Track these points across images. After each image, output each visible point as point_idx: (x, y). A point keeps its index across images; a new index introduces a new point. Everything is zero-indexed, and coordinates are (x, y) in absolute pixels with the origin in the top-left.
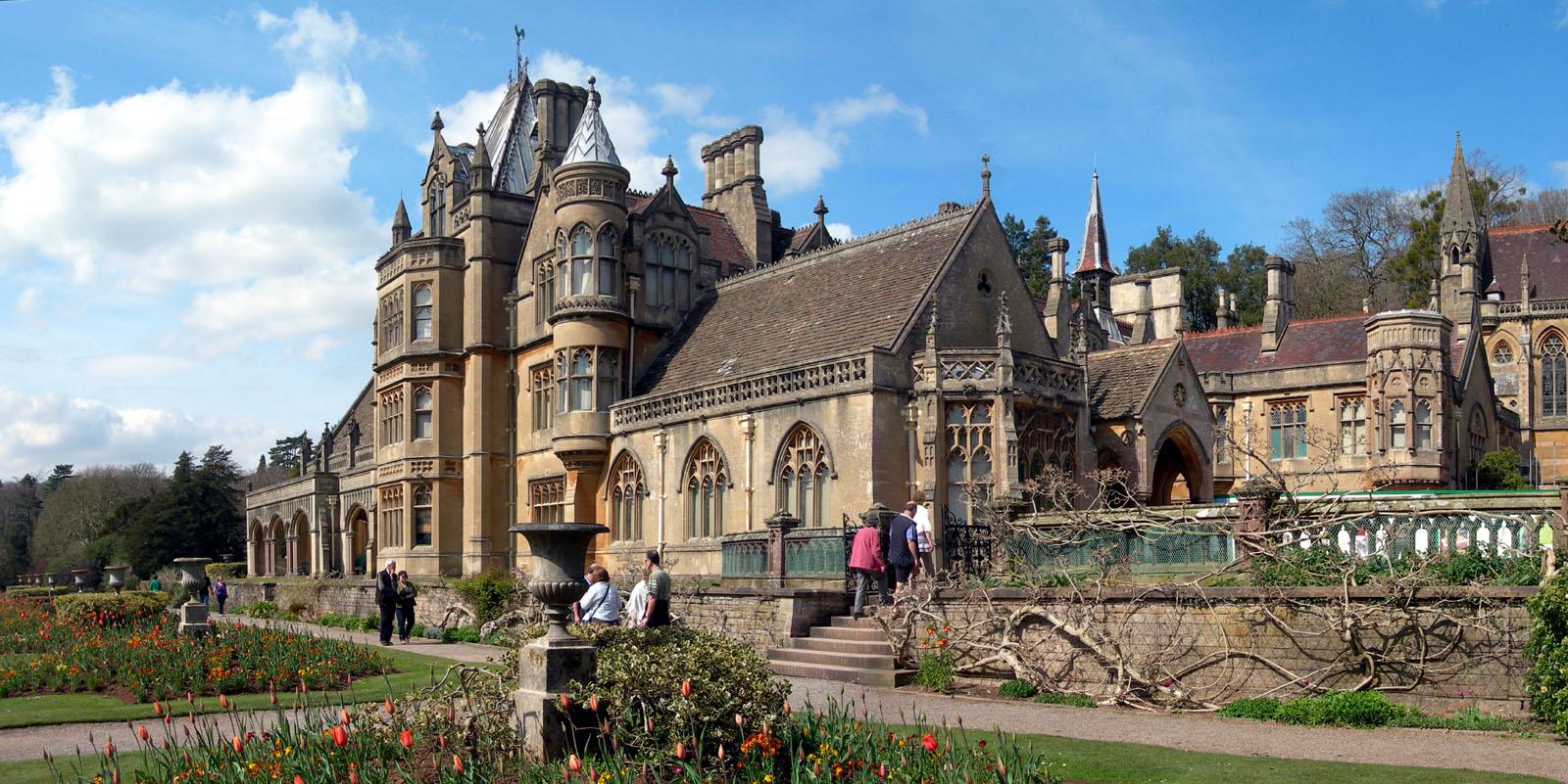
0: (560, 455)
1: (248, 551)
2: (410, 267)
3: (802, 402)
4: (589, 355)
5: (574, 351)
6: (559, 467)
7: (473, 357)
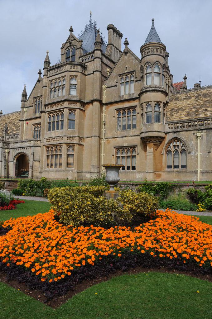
2: (69, 70)
4: (160, 105)
5: (155, 103)
7: (95, 103)
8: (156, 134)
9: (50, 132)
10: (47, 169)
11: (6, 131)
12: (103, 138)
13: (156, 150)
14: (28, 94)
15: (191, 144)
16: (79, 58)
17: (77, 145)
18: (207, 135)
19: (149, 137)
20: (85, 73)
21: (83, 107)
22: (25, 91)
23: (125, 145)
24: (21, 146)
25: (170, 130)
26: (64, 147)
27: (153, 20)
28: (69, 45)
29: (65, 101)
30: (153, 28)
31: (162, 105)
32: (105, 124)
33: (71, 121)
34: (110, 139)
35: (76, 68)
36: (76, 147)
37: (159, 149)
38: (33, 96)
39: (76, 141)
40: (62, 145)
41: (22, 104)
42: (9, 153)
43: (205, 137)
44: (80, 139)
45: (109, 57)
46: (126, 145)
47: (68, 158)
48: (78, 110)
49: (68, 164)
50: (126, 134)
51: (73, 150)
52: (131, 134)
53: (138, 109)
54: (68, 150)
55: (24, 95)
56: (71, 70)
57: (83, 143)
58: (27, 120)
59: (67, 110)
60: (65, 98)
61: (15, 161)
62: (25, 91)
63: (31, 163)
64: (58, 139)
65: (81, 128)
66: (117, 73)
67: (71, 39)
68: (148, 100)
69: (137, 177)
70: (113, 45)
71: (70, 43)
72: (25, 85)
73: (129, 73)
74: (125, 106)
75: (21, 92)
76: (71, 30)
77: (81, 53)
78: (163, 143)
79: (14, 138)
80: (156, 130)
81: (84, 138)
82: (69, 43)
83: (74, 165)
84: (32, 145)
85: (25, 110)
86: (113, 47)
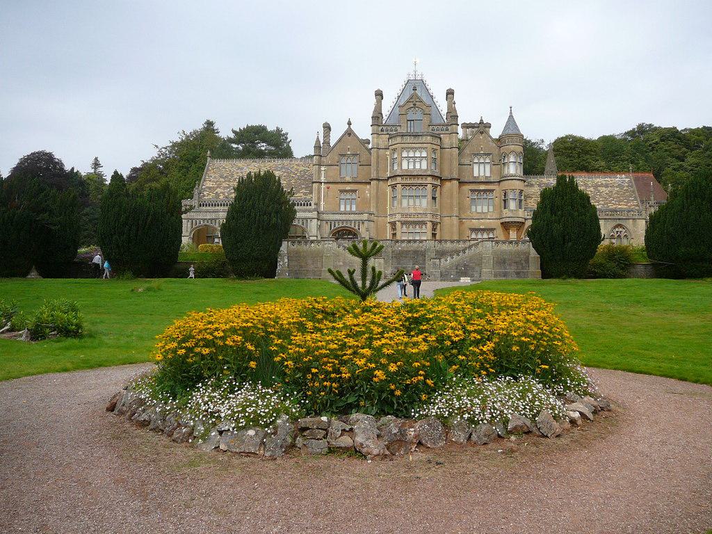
28: (412, 106)
30: (511, 117)
50: (483, 217)
52: (489, 217)
71: (415, 105)
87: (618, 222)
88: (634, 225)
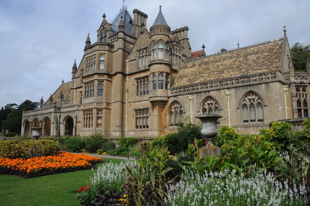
0: (151, 102)
1: (22, 130)
3: (250, 86)
4: (163, 74)
5: (159, 73)
6: (149, 105)
7: (118, 75)
8: (159, 99)
9: (85, 99)
10: (83, 129)
11: (61, 98)
12: (127, 102)
13: (162, 111)
14: (78, 68)
15: (186, 105)
16: (109, 38)
17: (105, 109)
18: (197, 98)
19: (157, 101)
20: (112, 51)
21: (111, 78)
22: (75, 64)
23: (141, 108)
24: (69, 111)
25: (171, 95)
26: (95, 111)
27: (160, 7)
28: (102, 28)
29: (95, 74)
30: (160, 13)
31: (164, 75)
32: (128, 91)
33: (100, 90)
34: (131, 103)
35: (104, 48)
36: (104, 110)
37: (164, 111)
38: (80, 69)
39: (104, 106)
40: (93, 110)
41: (73, 76)
42: (60, 116)
43: (195, 99)
44: (107, 104)
45: (133, 36)
46: (142, 108)
47: (97, 120)
48: (105, 81)
49: (97, 125)
50: (142, 99)
51: (102, 113)
52: (146, 99)
53: (151, 79)
54: (98, 113)
55: (75, 68)
56: (100, 49)
57: (109, 107)
58: (76, 89)
59: (97, 81)
60: (95, 72)
61: (65, 123)
62: (75, 64)
63: (75, 125)
64: (90, 105)
65: (108, 95)
66: (136, 50)
67: (104, 23)
68: (153, 72)
69: (149, 134)
70: (137, 26)
71: (103, 27)
72: (75, 59)
73: (144, 49)
74: (141, 76)
75: (72, 66)
76: (104, 16)
77: (110, 35)
78: (167, 105)
79: (67, 103)
80: (160, 95)
81: (111, 103)
82: (102, 27)
83: (102, 125)
84: (75, 109)
85: (75, 80)
86: (137, 27)
87: (249, 89)
88: (267, 89)
